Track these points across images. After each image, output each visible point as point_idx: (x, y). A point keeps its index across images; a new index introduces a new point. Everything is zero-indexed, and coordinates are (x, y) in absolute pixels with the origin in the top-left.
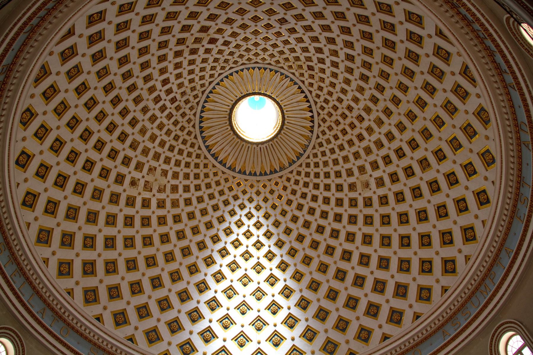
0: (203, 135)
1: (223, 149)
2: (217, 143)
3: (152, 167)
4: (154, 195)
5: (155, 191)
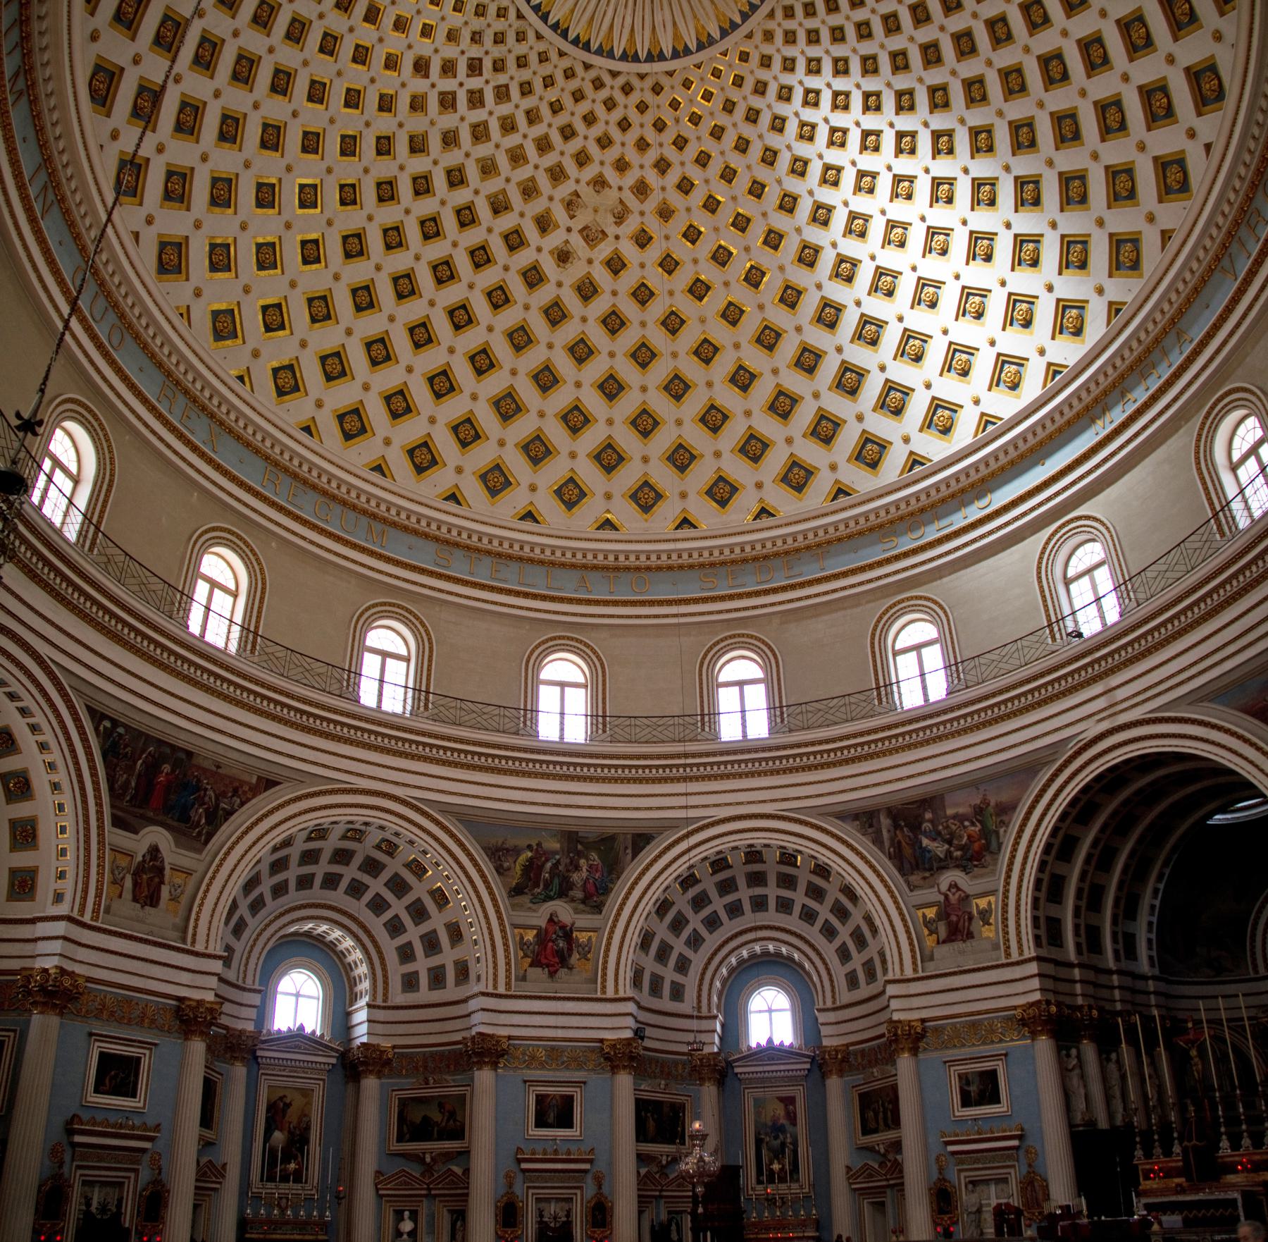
0: (594, 46)
1: (654, 28)
2: (632, 30)
3: (568, 198)
4: (617, 237)
5: (611, 230)
